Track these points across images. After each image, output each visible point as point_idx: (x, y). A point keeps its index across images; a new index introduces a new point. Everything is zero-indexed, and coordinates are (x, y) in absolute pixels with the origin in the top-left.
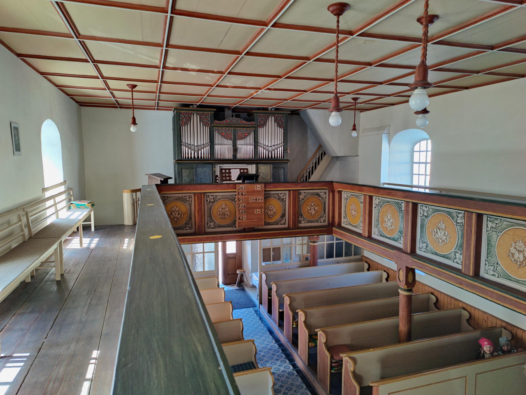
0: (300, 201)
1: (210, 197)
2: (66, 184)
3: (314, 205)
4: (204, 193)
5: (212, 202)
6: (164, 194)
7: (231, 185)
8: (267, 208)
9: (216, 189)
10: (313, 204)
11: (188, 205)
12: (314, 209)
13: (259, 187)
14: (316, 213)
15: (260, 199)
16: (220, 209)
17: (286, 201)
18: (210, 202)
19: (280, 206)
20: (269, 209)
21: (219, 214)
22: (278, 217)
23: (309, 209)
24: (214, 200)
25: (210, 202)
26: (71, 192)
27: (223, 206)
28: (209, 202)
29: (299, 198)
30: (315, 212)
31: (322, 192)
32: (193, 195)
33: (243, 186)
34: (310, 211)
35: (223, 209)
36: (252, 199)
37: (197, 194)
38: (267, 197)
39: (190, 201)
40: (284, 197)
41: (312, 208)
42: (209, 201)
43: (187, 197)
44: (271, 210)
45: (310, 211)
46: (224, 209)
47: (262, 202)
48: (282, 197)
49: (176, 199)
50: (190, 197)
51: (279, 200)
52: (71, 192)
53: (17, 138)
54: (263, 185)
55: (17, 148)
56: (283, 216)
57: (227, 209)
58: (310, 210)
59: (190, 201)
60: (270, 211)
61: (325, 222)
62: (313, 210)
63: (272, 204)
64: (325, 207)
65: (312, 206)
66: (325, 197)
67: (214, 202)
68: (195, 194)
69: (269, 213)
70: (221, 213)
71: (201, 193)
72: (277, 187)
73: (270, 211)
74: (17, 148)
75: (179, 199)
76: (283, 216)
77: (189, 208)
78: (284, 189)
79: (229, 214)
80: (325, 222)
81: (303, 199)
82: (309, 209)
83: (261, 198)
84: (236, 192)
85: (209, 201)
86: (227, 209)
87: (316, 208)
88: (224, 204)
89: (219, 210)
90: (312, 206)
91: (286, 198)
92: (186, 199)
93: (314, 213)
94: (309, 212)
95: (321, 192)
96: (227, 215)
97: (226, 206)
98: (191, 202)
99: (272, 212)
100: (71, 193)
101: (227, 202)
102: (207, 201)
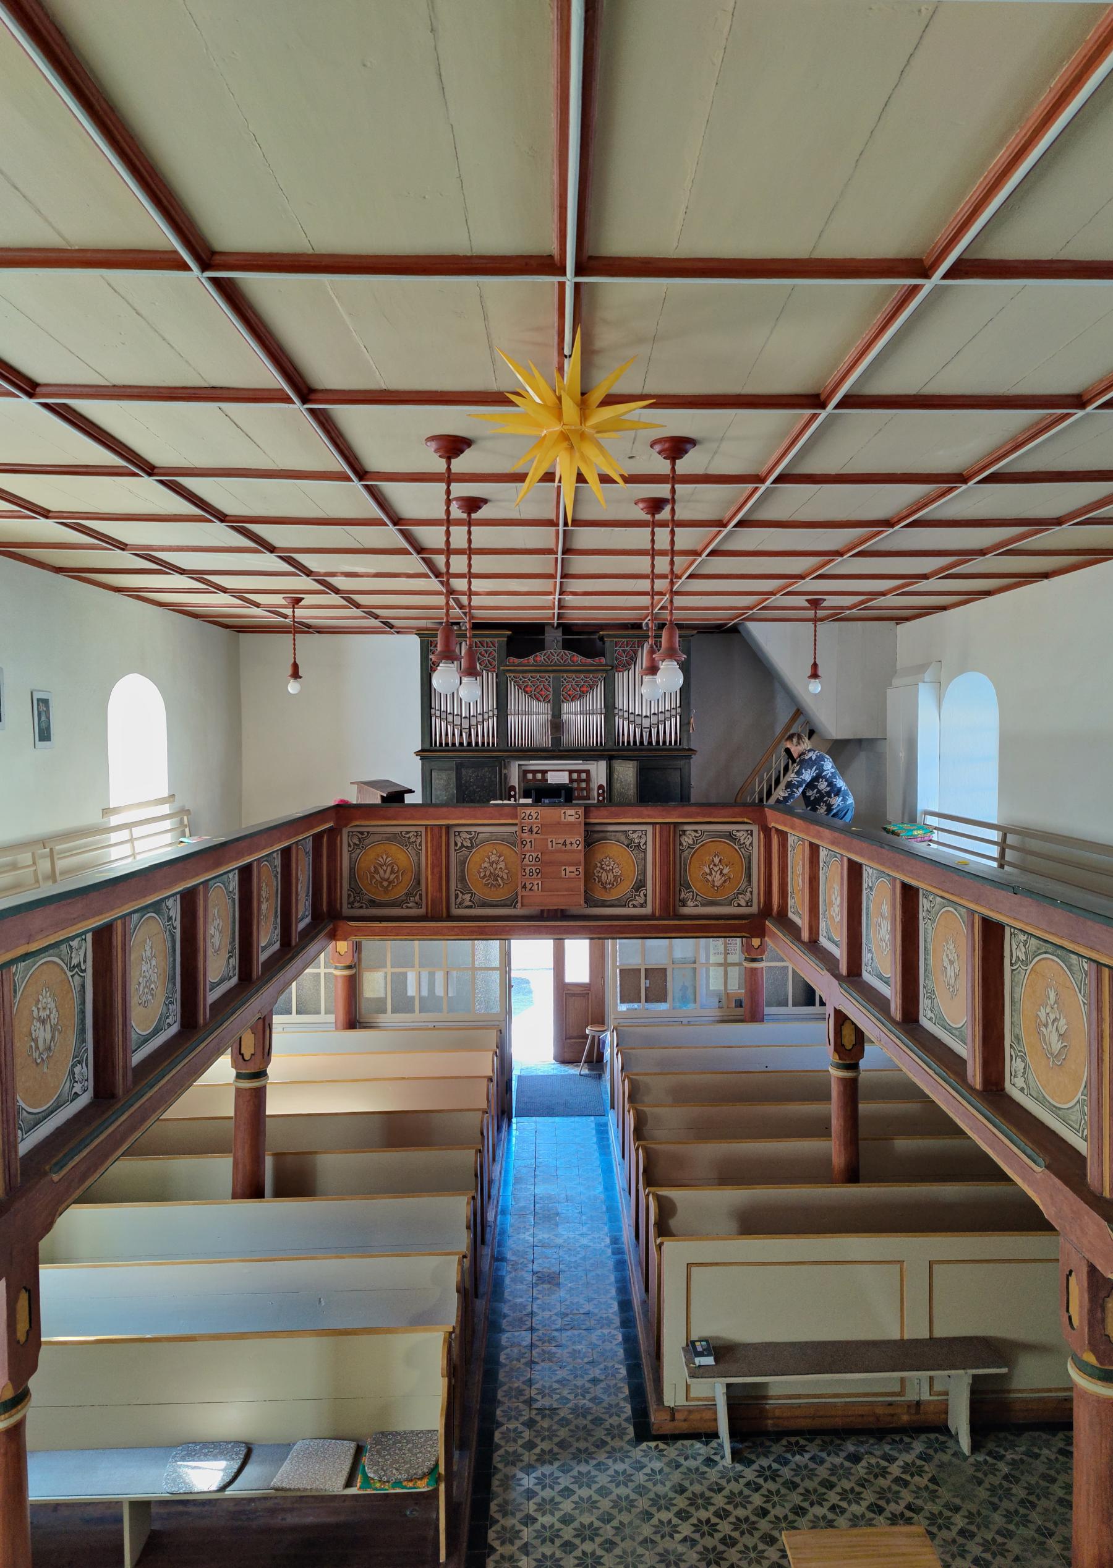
0: (682, 851)
1: (461, 835)
2: (174, 801)
3: (720, 861)
4: (448, 827)
5: (467, 847)
6: (357, 826)
7: (507, 810)
8: (599, 865)
9: (470, 819)
10: (717, 860)
11: (413, 852)
12: (721, 873)
13: (571, 814)
14: (725, 882)
15: (574, 842)
16: (486, 865)
17: (646, 849)
18: (463, 846)
19: (630, 861)
20: (602, 869)
21: (482, 874)
22: (625, 888)
23: (708, 871)
24: (471, 843)
25: (463, 846)
26: (185, 818)
27: (493, 858)
28: (460, 848)
29: (681, 844)
30: (723, 878)
31: (740, 831)
32: (423, 829)
33: (533, 811)
34: (708, 877)
35: (491, 864)
36: (554, 841)
37: (432, 829)
38: (592, 838)
39: (418, 843)
40: (643, 841)
41: (716, 869)
42: (459, 844)
43: (411, 834)
44: (609, 872)
45: (708, 877)
46: (494, 865)
47: (580, 851)
48: (636, 841)
49: (388, 839)
50: (417, 834)
51: (627, 846)
52: (185, 818)
53: (43, 718)
54: (581, 811)
55: (44, 735)
56: (640, 885)
57: (502, 865)
58: (711, 874)
59: (418, 843)
60: (607, 872)
61: (751, 906)
62: (718, 876)
63: (611, 855)
64: (749, 868)
65: (715, 865)
66: (751, 844)
67: (472, 847)
68: (426, 826)
69: (604, 877)
70: (488, 873)
71: (440, 826)
72: (617, 815)
73: (607, 872)
74: (44, 735)
75: (394, 838)
76: (640, 885)
77: (416, 858)
78: (636, 820)
79: (505, 877)
80: (751, 906)
81: (690, 847)
82: (708, 871)
83: (576, 840)
84: (516, 824)
85: (459, 844)
86: (502, 865)
87: (725, 872)
88: (495, 852)
89: (483, 865)
90: (715, 865)
91: (645, 843)
92: (409, 838)
93: (721, 881)
94: (707, 880)
95: (738, 831)
96: (502, 878)
97: (499, 857)
98: (420, 845)
99: (611, 877)
100: (186, 822)
101: (502, 847)
102: (456, 844)
